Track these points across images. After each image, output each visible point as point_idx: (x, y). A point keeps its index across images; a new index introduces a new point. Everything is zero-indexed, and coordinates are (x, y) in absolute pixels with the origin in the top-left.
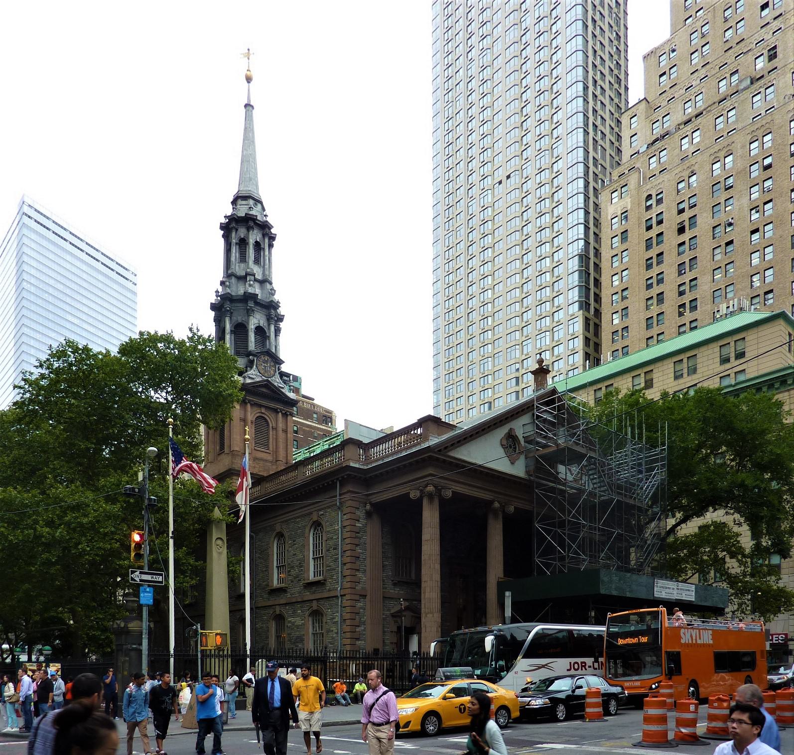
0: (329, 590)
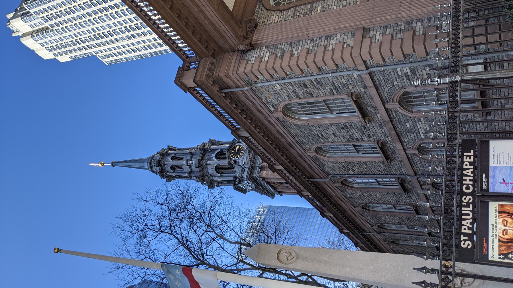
0: (365, 87)
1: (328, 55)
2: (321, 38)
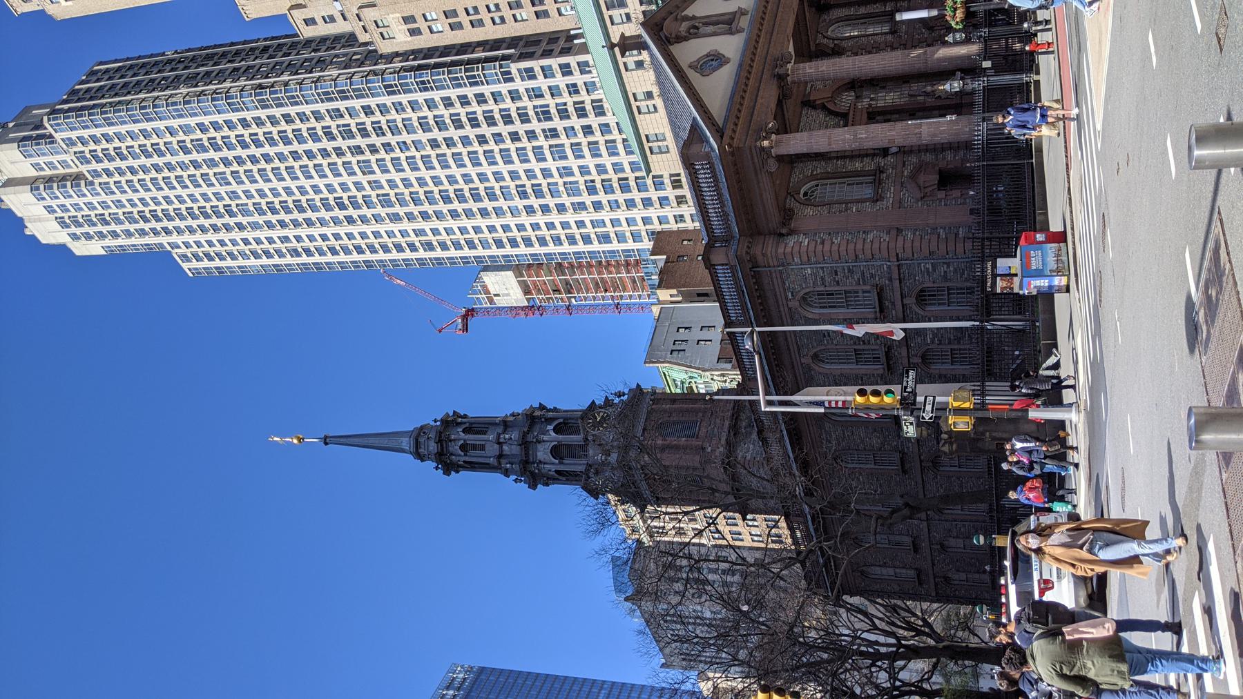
0: (890, 280)
1: (868, 246)
2: (859, 232)
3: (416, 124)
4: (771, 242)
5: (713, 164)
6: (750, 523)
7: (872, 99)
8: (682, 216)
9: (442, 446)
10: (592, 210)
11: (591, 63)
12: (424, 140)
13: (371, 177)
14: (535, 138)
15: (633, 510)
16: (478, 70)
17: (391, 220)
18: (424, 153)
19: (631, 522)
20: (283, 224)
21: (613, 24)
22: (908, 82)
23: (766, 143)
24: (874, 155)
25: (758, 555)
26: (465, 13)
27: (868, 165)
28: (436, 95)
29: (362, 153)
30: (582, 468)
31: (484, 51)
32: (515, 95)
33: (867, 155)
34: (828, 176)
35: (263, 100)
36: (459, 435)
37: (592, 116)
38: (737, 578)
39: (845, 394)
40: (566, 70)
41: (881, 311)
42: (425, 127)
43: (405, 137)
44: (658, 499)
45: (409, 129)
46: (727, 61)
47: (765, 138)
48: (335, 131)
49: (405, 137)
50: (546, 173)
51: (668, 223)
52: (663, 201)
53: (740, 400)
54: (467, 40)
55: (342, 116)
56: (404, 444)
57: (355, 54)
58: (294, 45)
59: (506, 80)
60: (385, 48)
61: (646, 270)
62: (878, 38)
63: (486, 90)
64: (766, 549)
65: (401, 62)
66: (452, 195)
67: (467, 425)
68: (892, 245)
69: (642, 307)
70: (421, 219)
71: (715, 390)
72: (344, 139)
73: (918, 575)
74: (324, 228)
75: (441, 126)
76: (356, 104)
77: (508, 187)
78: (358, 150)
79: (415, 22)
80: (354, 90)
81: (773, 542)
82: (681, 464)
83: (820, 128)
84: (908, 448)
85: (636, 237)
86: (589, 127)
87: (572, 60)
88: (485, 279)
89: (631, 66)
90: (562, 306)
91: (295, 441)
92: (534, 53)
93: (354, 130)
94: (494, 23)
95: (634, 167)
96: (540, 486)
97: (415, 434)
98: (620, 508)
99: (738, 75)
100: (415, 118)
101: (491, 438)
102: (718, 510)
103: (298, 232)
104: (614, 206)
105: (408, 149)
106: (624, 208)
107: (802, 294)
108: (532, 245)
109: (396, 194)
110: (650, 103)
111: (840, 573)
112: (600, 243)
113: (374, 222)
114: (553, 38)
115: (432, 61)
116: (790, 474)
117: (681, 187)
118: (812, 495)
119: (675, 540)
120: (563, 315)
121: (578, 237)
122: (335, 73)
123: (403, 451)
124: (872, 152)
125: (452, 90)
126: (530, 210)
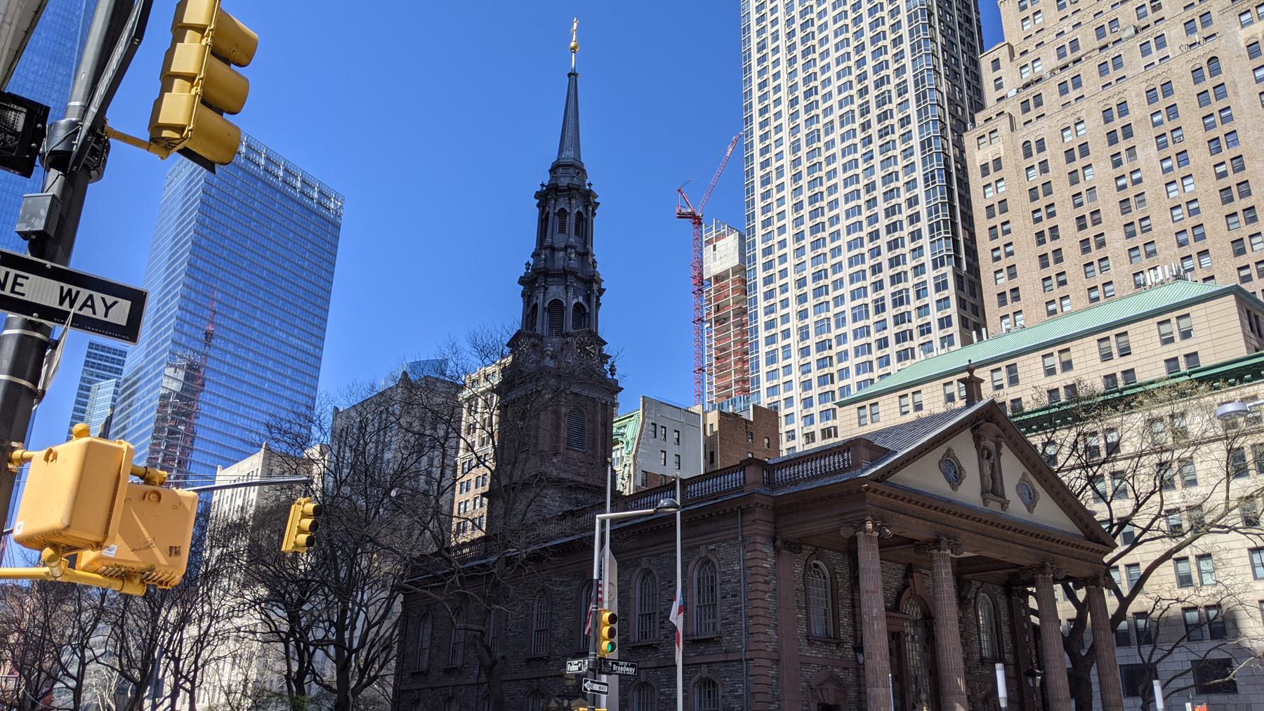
0: (727, 652)
1: (761, 629)
3: (891, 170)
4: (767, 529)
5: (849, 471)
6: (478, 501)
7: (913, 637)
8: (793, 438)
9: (564, 191)
10: (801, 346)
11: (952, 348)
12: (874, 178)
13: (837, 124)
14: (876, 290)
15: (496, 381)
16: (945, 233)
17: (793, 143)
18: (861, 177)
19: (482, 379)
20: (791, 35)
21: (993, 371)
22: (930, 674)
23: (869, 526)
24: (855, 637)
25: (446, 508)
26: (1004, 220)
27: (845, 631)
28: (920, 190)
29: (862, 115)
30: (538, 331)
31: (965, 239)
32: (919, 269)
33: (855, 630)
34: (834, 587)
35: (916, 17)
36: (576, 207)
37: (898, 348)
38: (423, 485)
39: (610, 602)
40: (945, 322)
41: (695, 642)
42: (887, 179)
43: (878, 158)
44: (507, 406)
45: (885, 163)
46: (954, 488)
47: (874, 525)
48: (884, 88)
49: (878, 158)
50: (839, 300)
51: (787, 424)
52: (809, 419)
53: (606, 493)
54: (976, 223)
55: (900, 95)
56: (568, 153)
57: (963, 109)
58: (973, 48)
59: (934, 261)
60: (969, 139)
61: (738, 400)
62: (976, 645)
63: (925, 241)
64: (451, 517)
65: (955, 155)
66: (817, 205)
67: (585, 216)
68: (762, 654)
69: (700, 395)
70: (793, 173)
71: (615, 468)
72: (877, 97)
73: (422, 672)
74: (786, 76)
75: (889, 195)
76: (912, 110)
77: (825, 261)
78: (865, 111)
79: (996, 170)
80: (926, 108)
81: (459, 524)
82: (541, 431)
83: (884, 582)
84: (552, 665)
85: (772, 390)
86: (886, 345)
87: (955, 329)
88: (732, 237)
89: (949, 389)
90: (702, 313)
91: (573, 44)
92: (963, 290)
93: (886, 107)
94: (994, 250)
95: (845, 390)
96: (522, 288)
97: (576, 163)
98: (497, 369)
99: (940, 499)
100: (896, 168)
101: (572, 240)
102: (493, 468)
103: (783, 50)
104: (805, 368)
105: (865, 161)
106: (803, 379)
107: (714, 560)
108: (765, 284)
109: (819, 148)
110: (911, 408)
111: (428, 592)
112: (767, 353)
113: (792, 126)
114: (979, 310)
115: (955, 187)
116: (530, 543)
117: (824, 437)
118: (507, 565)
119: (463, 423)
120: (693, 315)
121: (773, 331)
122: (944, 89)
123: (561, 151)
124: (859, 635)
125: (925, 206)
126: (801, 283)
